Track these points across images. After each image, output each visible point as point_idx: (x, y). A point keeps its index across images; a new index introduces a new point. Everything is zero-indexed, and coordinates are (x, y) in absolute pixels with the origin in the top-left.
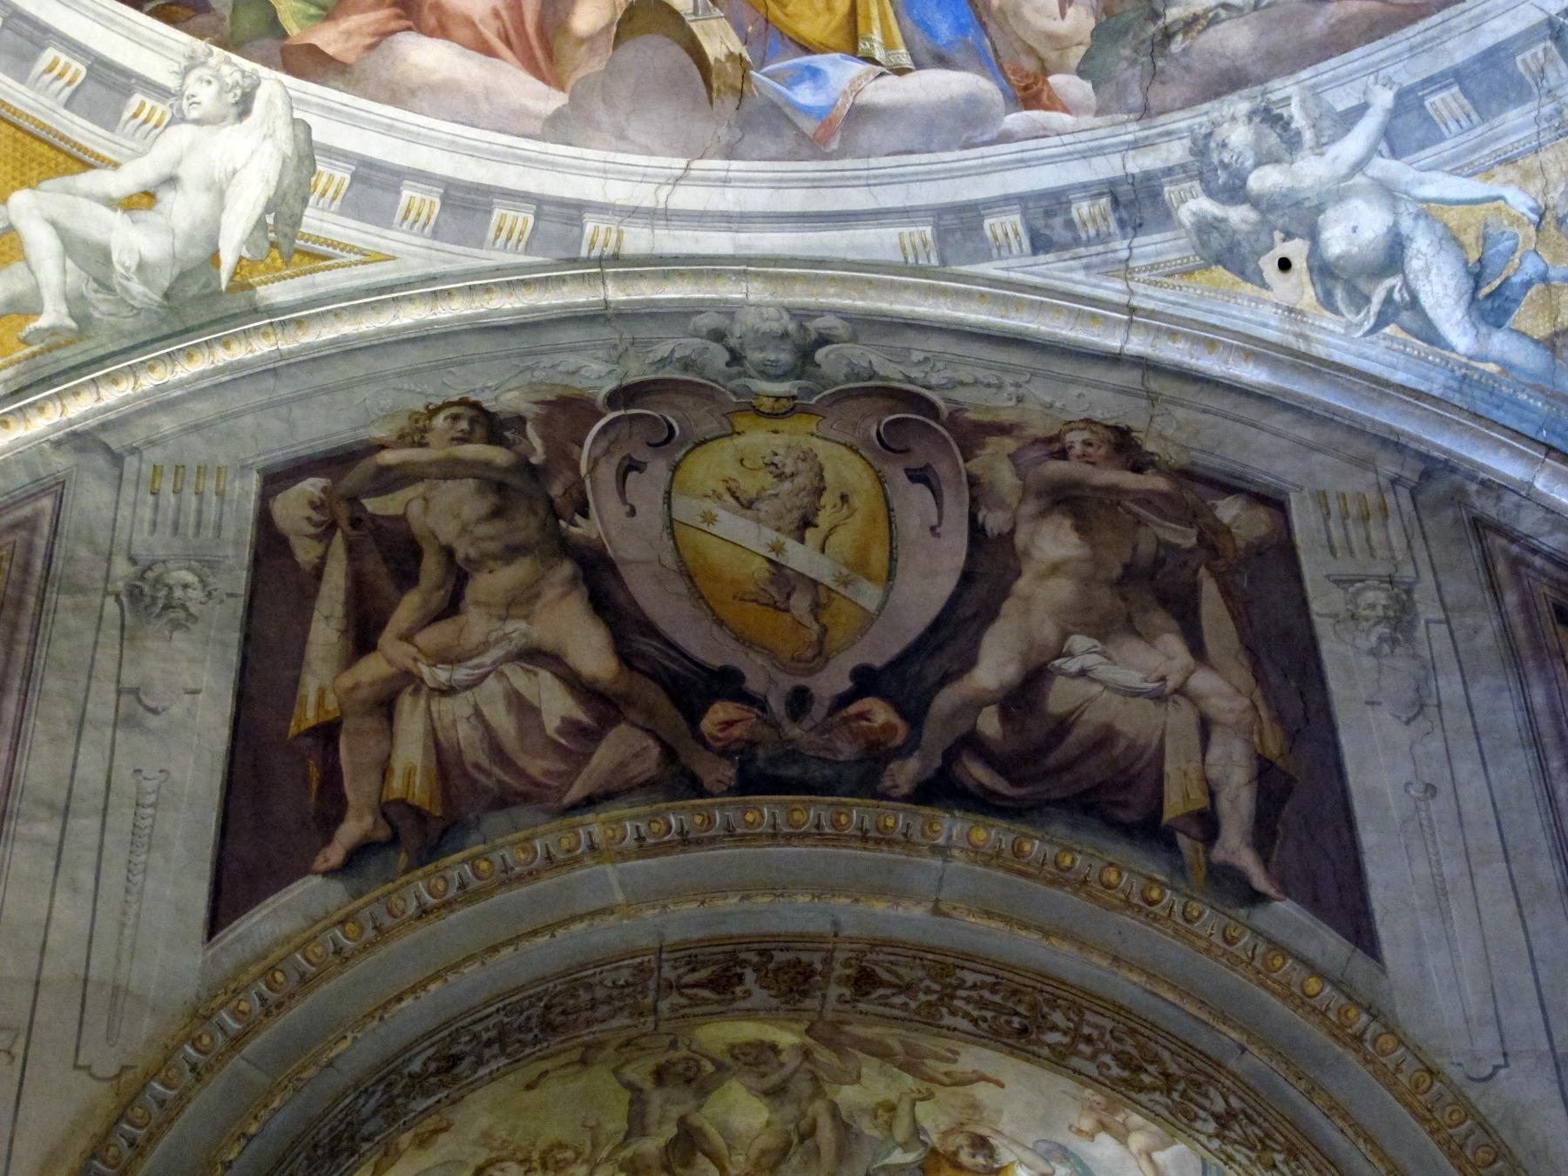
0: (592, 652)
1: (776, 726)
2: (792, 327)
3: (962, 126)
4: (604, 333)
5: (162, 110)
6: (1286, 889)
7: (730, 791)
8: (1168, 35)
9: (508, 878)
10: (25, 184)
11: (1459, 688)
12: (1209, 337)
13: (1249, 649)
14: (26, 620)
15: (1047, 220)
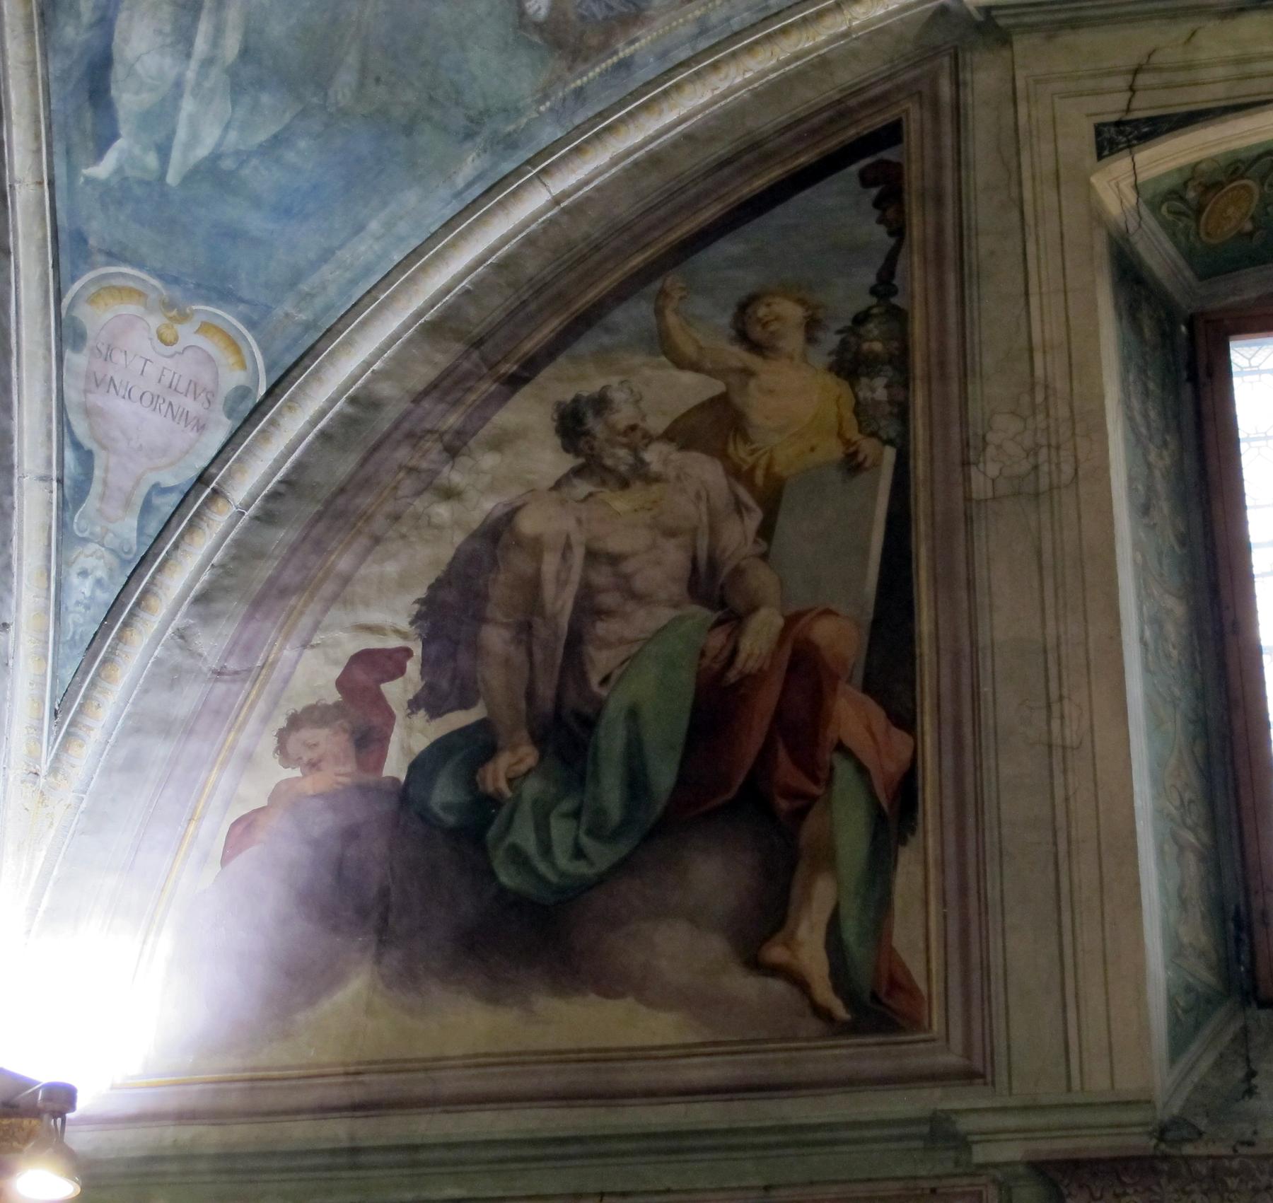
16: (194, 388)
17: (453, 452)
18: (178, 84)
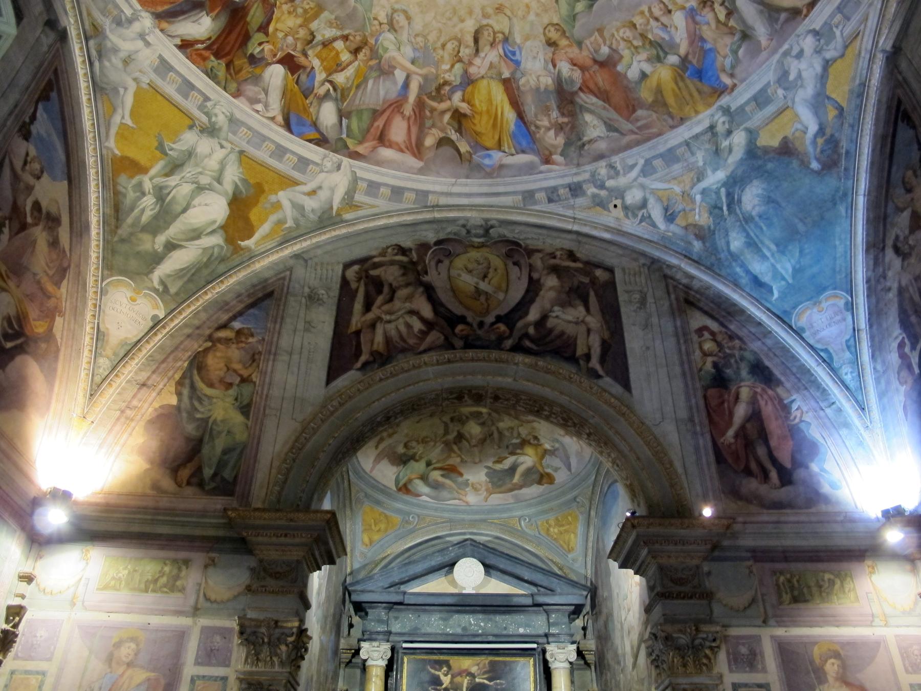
0: (427, 311)
1: (474, 331)
2: (483, 223)
3: (530, 169)
4: (435, 226)
5: (318, 169)
6: (607, 374)
7: (461, 348)
8: (584, 145)
9: (404, 371)
10: (282, 189)
11: (657, 320)
12: (595, 226)
13: (602, 310)
14: (282, 304)
15: (552, 195)
16: (836, 314)
17: (885, 278)
18: (773, 265)
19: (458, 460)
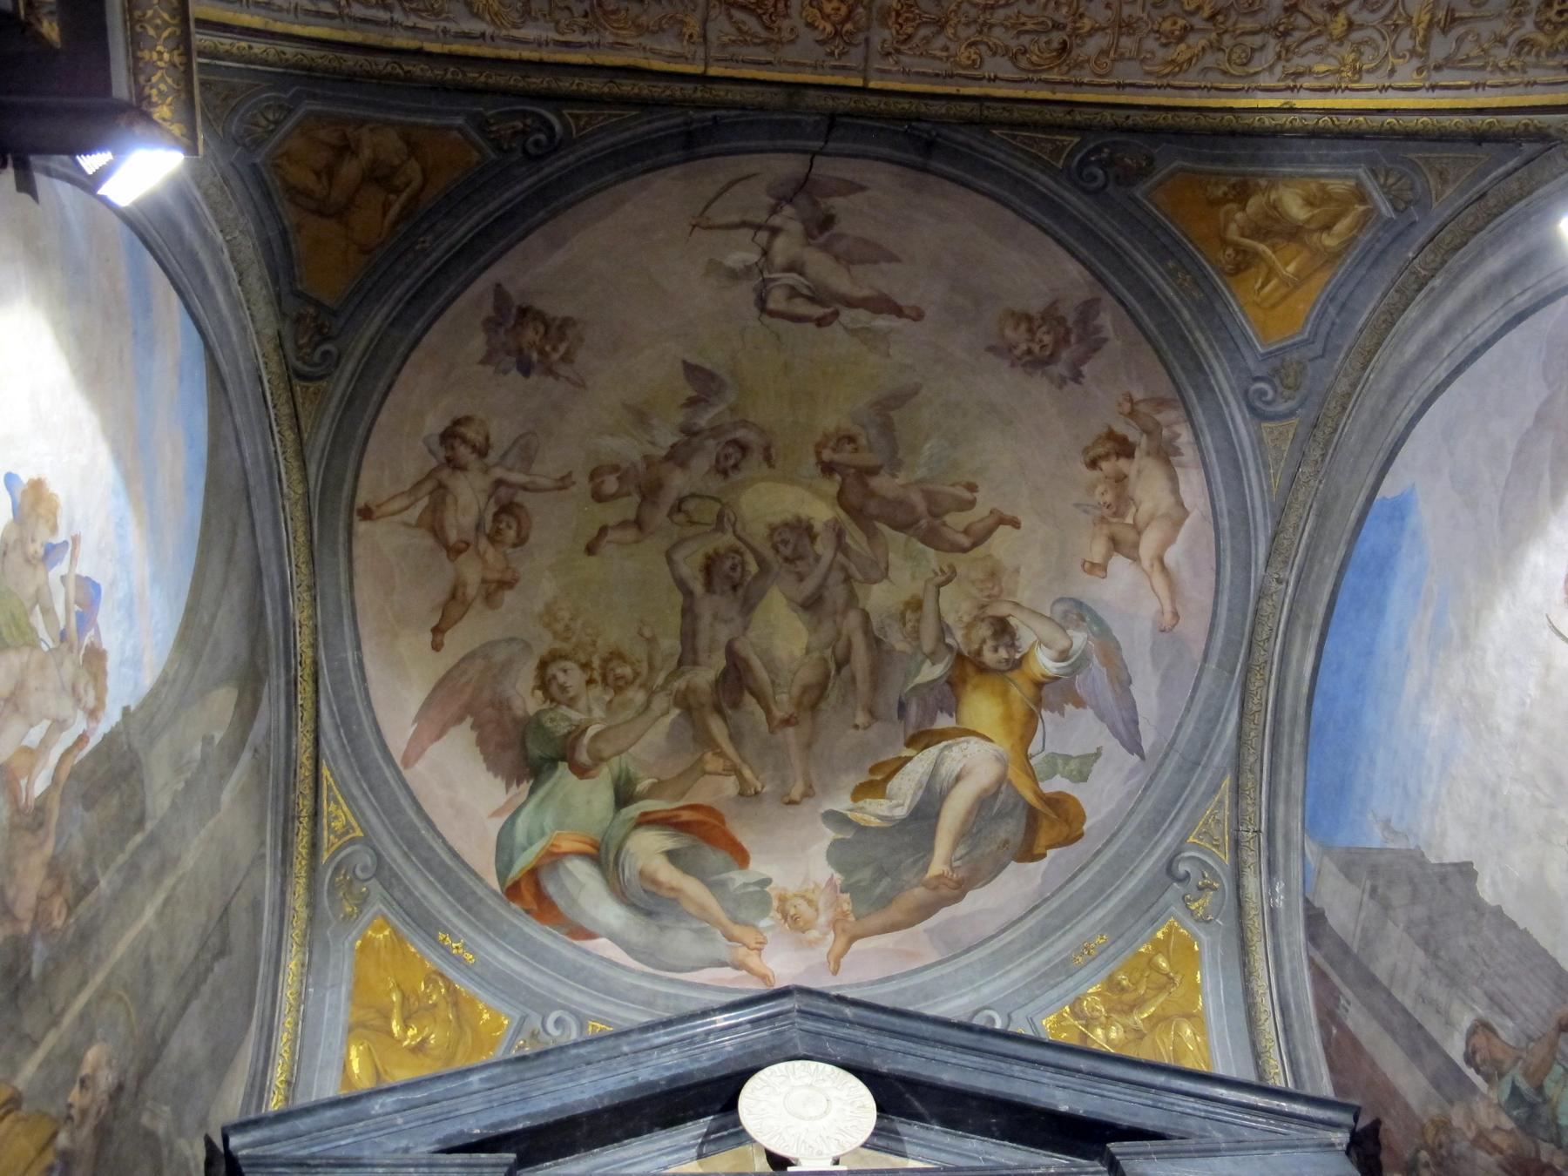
19: (730, 785)
